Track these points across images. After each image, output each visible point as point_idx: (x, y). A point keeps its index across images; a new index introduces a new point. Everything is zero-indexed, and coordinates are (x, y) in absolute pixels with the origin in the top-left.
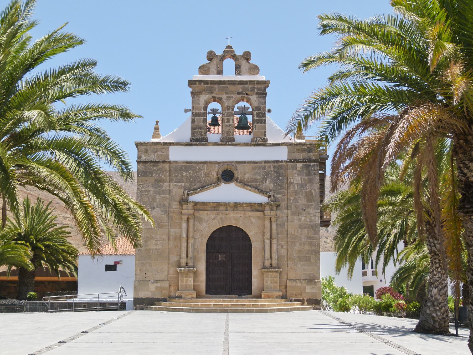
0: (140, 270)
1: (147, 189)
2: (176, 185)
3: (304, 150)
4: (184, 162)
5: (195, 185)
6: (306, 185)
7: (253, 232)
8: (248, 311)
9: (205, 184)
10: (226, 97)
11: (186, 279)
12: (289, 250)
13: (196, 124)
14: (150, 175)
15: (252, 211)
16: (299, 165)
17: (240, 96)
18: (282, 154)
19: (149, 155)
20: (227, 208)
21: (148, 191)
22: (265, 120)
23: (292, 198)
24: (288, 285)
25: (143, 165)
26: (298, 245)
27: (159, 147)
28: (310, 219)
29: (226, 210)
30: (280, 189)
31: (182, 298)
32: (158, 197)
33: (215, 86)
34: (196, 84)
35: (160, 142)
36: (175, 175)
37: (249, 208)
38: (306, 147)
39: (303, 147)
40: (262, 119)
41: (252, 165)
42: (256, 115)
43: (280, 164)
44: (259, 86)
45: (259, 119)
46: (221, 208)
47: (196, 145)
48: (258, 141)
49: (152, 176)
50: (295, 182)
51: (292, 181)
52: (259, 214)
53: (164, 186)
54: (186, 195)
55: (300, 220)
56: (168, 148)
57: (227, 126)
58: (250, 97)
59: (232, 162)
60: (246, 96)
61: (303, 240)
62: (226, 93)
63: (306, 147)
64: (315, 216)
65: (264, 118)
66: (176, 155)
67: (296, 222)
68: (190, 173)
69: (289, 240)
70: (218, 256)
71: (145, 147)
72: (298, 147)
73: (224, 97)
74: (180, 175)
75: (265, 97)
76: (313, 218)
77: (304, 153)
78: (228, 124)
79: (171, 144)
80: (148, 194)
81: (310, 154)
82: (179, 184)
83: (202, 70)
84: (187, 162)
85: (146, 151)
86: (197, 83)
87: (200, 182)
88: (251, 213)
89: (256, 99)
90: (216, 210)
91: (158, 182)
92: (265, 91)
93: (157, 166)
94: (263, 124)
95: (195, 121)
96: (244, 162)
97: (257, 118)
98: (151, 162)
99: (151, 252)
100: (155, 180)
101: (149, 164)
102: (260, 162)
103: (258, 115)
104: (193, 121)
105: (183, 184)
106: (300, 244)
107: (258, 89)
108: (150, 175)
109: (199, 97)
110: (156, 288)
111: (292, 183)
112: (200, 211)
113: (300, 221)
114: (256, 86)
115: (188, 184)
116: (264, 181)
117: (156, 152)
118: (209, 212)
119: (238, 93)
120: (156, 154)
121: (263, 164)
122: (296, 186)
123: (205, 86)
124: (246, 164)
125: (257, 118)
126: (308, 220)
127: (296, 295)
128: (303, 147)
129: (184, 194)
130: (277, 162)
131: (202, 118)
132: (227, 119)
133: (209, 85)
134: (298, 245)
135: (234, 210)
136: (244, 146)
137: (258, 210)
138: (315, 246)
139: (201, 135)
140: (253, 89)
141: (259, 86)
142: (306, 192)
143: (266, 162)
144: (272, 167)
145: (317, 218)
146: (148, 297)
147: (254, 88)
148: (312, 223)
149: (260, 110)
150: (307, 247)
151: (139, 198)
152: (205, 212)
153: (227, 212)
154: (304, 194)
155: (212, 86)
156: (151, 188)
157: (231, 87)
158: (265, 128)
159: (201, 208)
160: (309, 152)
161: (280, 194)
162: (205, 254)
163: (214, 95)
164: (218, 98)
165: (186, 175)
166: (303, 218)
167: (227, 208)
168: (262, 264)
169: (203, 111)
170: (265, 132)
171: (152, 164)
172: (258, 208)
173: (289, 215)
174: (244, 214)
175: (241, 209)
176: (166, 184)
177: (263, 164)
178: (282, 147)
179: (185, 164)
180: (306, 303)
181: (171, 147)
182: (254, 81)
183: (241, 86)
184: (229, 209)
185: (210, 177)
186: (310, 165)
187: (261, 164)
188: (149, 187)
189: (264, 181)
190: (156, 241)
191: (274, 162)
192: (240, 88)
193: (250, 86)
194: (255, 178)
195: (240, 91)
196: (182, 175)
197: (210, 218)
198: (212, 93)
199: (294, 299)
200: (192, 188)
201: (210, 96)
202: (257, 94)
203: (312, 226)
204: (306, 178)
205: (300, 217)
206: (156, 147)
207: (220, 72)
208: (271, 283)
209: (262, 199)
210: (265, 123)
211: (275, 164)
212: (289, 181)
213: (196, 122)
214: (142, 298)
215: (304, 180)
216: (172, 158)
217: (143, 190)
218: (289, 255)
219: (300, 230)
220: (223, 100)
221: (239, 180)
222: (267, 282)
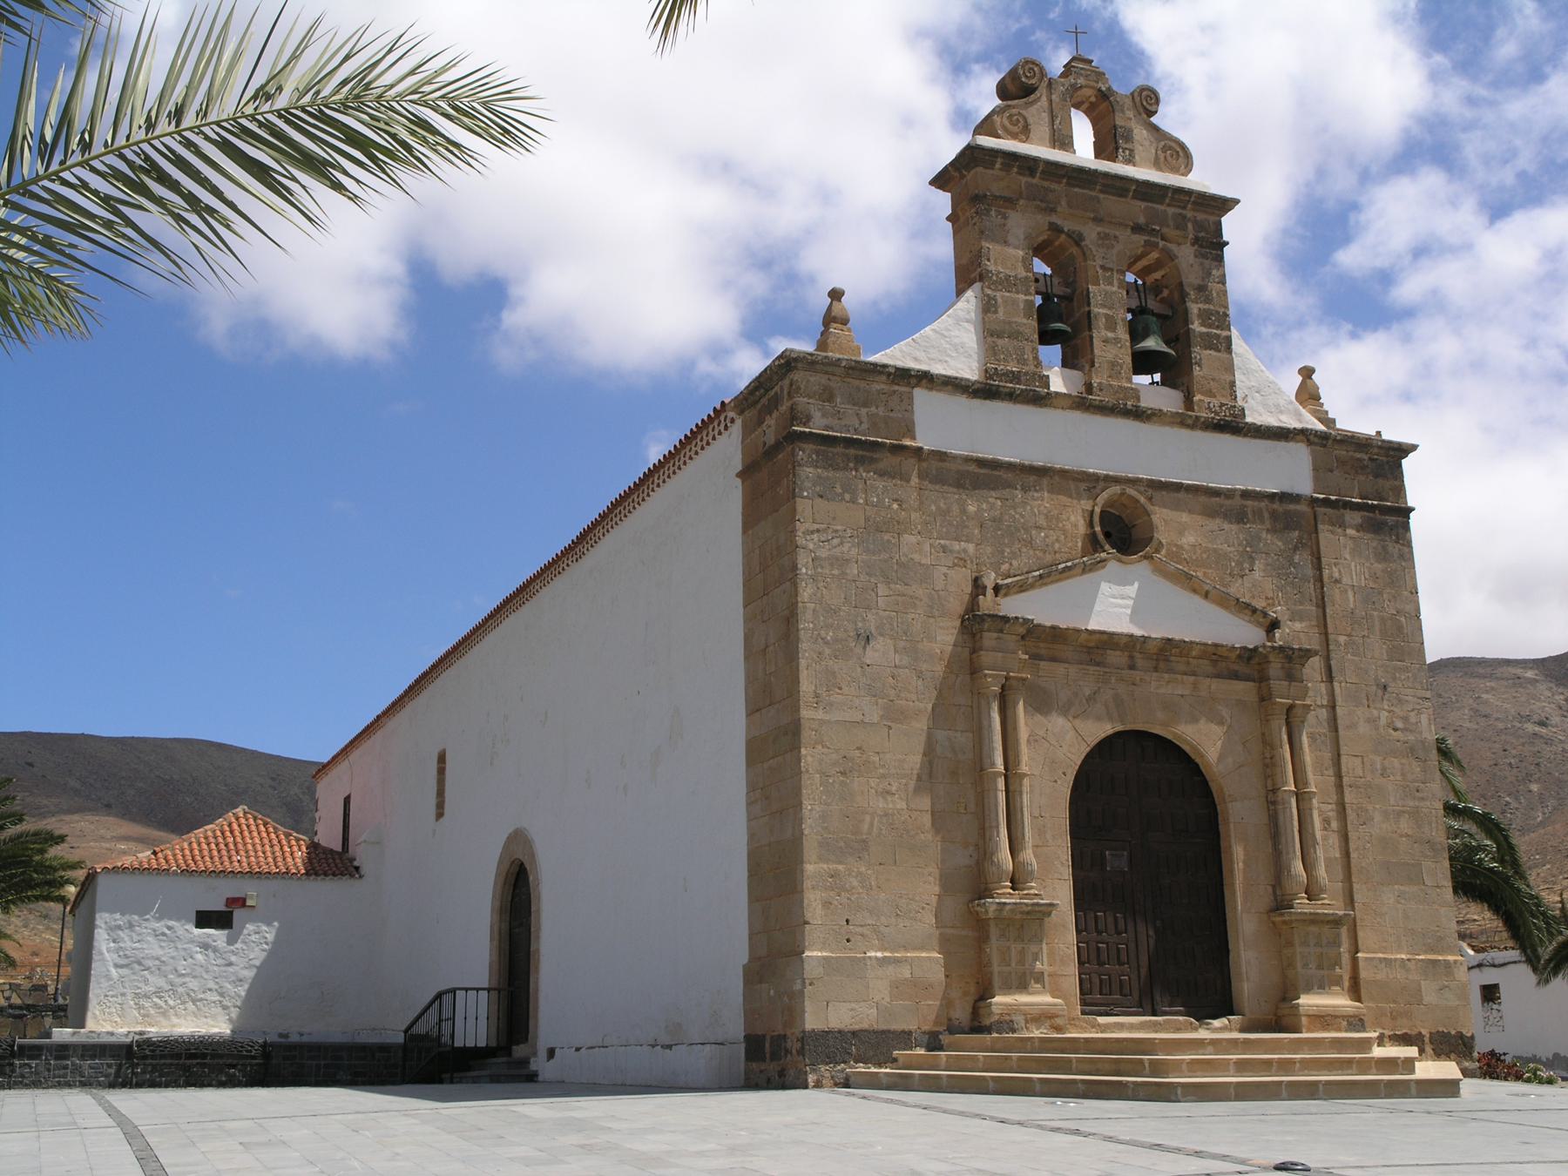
0: (827, 904)
1: (837, 552)
2: (944, 549)
3: (1359, 467)
4: (968, 460)
5: (1014, 555)
6: (1380, 593)
7: (1230, 760)
8: (1309, 1091)
9: (1049, 558)
10: (1094, 235)
11: (1019, 947)
12: (1352, 835)
13: (1001, 315)
14: (847, 497)
15: (1218, 676)
16: (1354, 517)
17: (1140, 239)
18: (1293, 472)
19: (838, 415)
20: (1131, 657)
21: (842, 562)
22: (1229, 340)
23: (1342, 639)
24: (1363, 974)
25: (818, 453)
26: (1378, 817)
27: (879, 385)
28: (1405, 719)
29: (1132, 667)
30: (1301, 604)
31: (1014, 1031)
32: (882, 590)
33: (1054, 186)
34: (991, 166)
35: (885, 366)
36: (938, 508)
37: (1205, 665)
38: (1366, 457)
39: (1358, 455)
40: (1218, 336)
41: (1203, 499)
42: (1199, 316)
43: (1292, 507)
44: (1201, 216)
45: (1208, 334)
46: (1115, 657)
47: (1011, 397)
48: (1216, 413)
49: (853, 501)
50: (1345, 580)
51: (1336, 575)
52: (1244, 690)
53: (904, 549)
54: (990, 592)
55: (1373, 721)
56: (911, 398)
57: (1106, 341)
58: (1173, 247)
59: (1134, 482)
60: (1162, 243)
61: (1392, 802)
62: (1098, 220)
63: (1366, 457)
64: (1419, 713)
65: (1225, 333)
66: (940, 426)
67: (1363, 728)
68: (992, 506)
69: (1349, 797)
70: (1103, 857)
71: (823, 379)
72: (1341, 452)
73: (1091, 233)
74: (955, 508)
75: (1220, 259)
76: (1413, 720)
77: (1362, 478)
78: (1110, 335)
79: (926, 379)
80: (844, 574)
81: (1380, 481)
82: (956, 546)
83: (1006, 123)
84: (981, 463)
85: (828, 396)
86: (998, 166)
87: (1030, 543)
88: (1217, 685)
89: (1191, 259)
90: (1098, 664)
91: (879, 530)
92: (1221, 235)
93: (873, 460)
94: (1223, 355)
95: (996, 306)
96: (1178, 487)
97: (1204, 330)
98: (849, 442)
99: (866, 827)
100: (867, 519)
101: (839, 449)
102: (1229, 494)
103: (1205, 317)
104: (988, 306)
105: (971, 547)
106: (1386, 814)
107: (1199, 226)
108: (847, 497)
109: (1005, 217)
110: (897, 986)
111: (1337, 581)
112: (1042, 663)
113: (1377, 729)
114: (1189, 214)
115: (989, 550)
116: (1246, 565)
117: (865, 405)
118: (1073, 670)
119: (1137, 229)
120: (864, 411)
121: (1238, 501)
122: (1350, 594)
123: (1024, 180)
124: (1182, 495)
125: (1204, 330)
126: (1399, 724)
127: (1394, 1018)
128: (1358, 455)
129: (978, 587)
130: (1284, 497)
131: (1022, 297)
132: (1107, 316)
133: (1035, 181)
134: (1378, 817)
135: (1156, 669)
136: (1172, 424)
137: (1235, 676)
138: (1430, 823)
139: (1021, 361)
140: (1181, 222)
141: (1201, 216)
142: (1383, 620)
143: (1246, 494)
144: (1266, 515)
145: (1424, 719)
146: (865, 1026)
147: (1184, 217)
148: (1411, 738)
149: (1208, 300)
150: (1405, 825)
151: (809, 590)
152: (1060, 669)
153: (1137, 675)
154: (1377, 628)
155: (1046, 184)
156: (849, 550)
157: (1110, 204)
158: (1230, 368)
159: (1043, 652)
160: (1376, 476)
161: (1301, 620)
162: (1066, 841)
163: (1054, 219)
164: (1069, 235)
165: (980, 510)
166: (1383, 721)
167: (1131, 657)
168: (1270, 889)
169: (1022, 273)
170: (1233, 384)
171: (852, 451)
172: (1236, 667)
173: (1339, 701)
174: (1195, 686)
175: (1182, 667)
176: (910, 539)
177: (1238, 501)
178: (1291, 445)
179: (972, 468)
180: (1429, 1049)
181: (920, 395)
182: (1189, 192)
183: (1143, 205)
184: (1140, 662)
185: (1065, 532)
186: (1384, 523)
187: (1228, 502)
188: (845, 549)
189: (1246, 565)
190: (883, 776)
191: (1272, 497)
192: (1138, 210)
193: (1171, 211)
194: (1215, 550)
195: (1142, 220)
196: (964, 511)
197: (1076, 694)
198: (1053, 210)
199: (1387, 1033)
200: (1005, 567)
201: (1043, 220)
202: (1196, 241)
203: (1412, 750)
204: (1378, 567)
205: (1375, 712)
206: (863, 384)
207: (1063, 140)
208: (1320, 967)
209: (1241, 633)
210: (1229, 349)
211: (1276, 506)
212: (1326, 573)
213: (1001, 311)
214: (840, 1032)
215: (1374, 576)
216: (925, 439)
217: (823, 553)
218: (1354, 855)
219: (1378, 759)
220: (1087, 242)
221: (1163, 552)
222: (1305, 965)
